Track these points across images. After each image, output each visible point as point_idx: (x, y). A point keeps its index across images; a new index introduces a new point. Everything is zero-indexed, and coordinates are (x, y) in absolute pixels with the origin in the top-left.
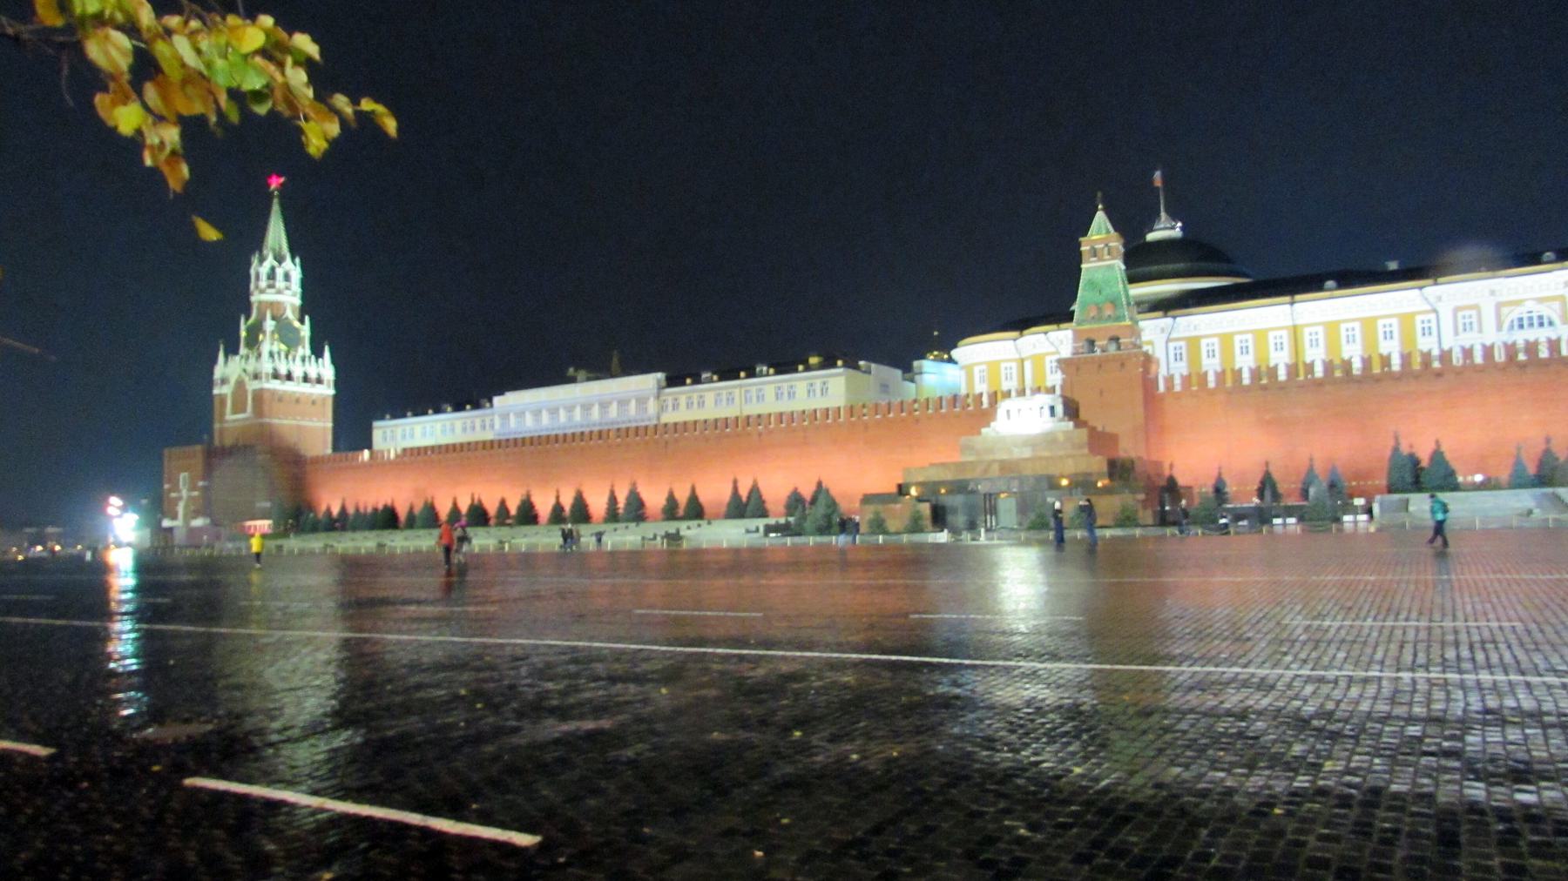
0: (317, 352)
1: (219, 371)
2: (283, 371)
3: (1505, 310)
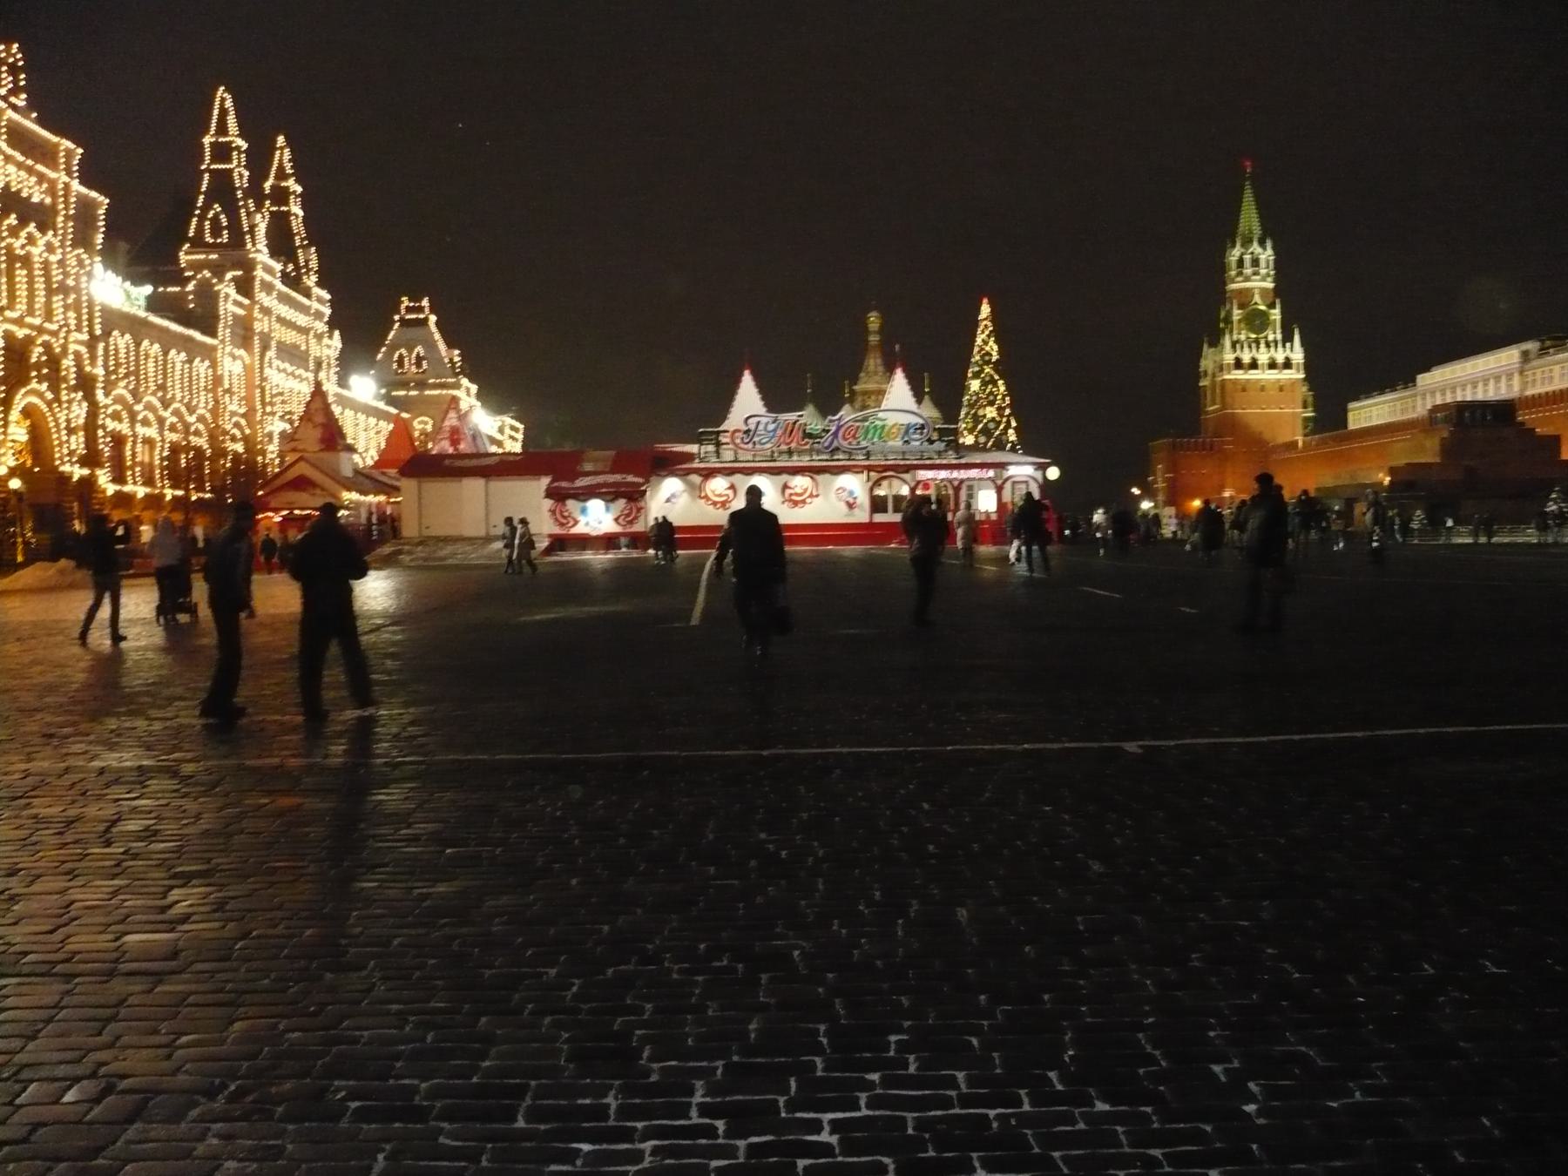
0: (1287, 338)
2: (1246, 358)
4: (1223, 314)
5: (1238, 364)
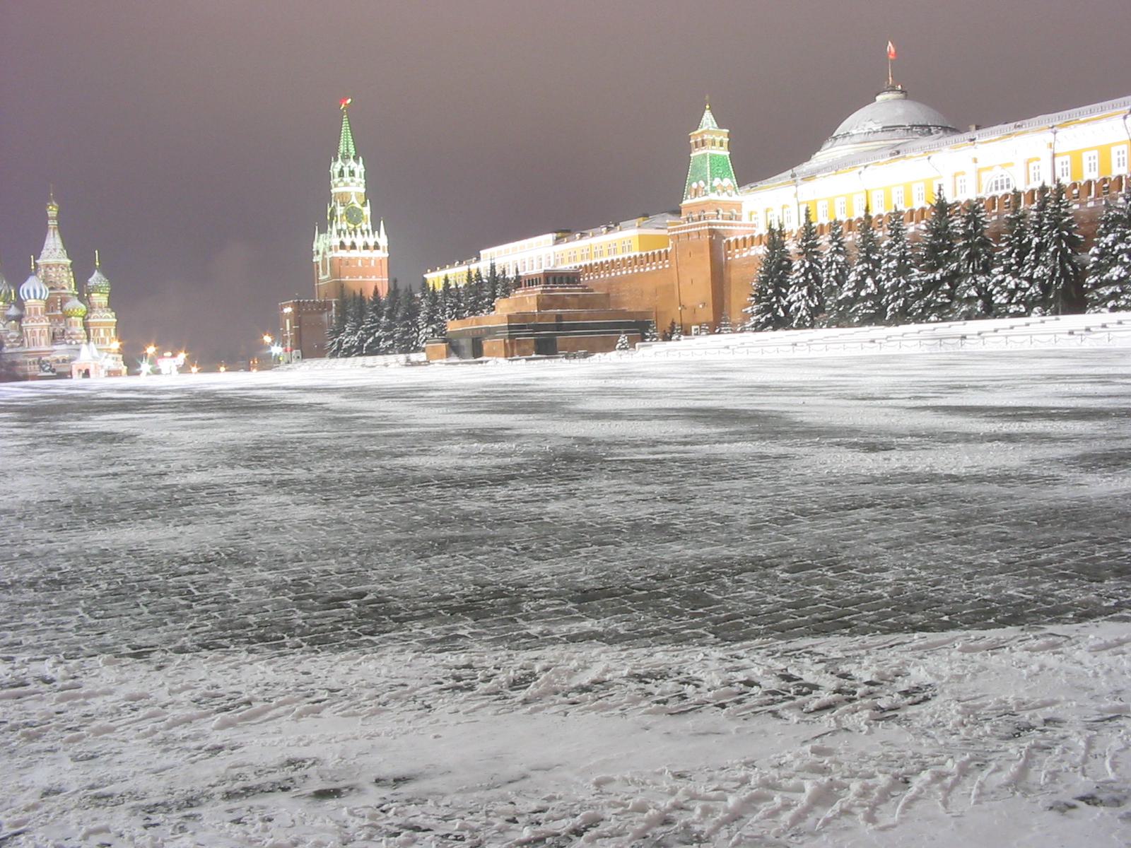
0: (376, 228)
1: (315, 246)
3: (984, 175)
4: (329, 211)
5: (342, 246)
